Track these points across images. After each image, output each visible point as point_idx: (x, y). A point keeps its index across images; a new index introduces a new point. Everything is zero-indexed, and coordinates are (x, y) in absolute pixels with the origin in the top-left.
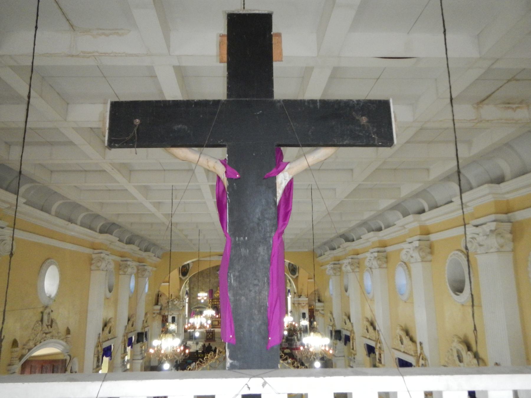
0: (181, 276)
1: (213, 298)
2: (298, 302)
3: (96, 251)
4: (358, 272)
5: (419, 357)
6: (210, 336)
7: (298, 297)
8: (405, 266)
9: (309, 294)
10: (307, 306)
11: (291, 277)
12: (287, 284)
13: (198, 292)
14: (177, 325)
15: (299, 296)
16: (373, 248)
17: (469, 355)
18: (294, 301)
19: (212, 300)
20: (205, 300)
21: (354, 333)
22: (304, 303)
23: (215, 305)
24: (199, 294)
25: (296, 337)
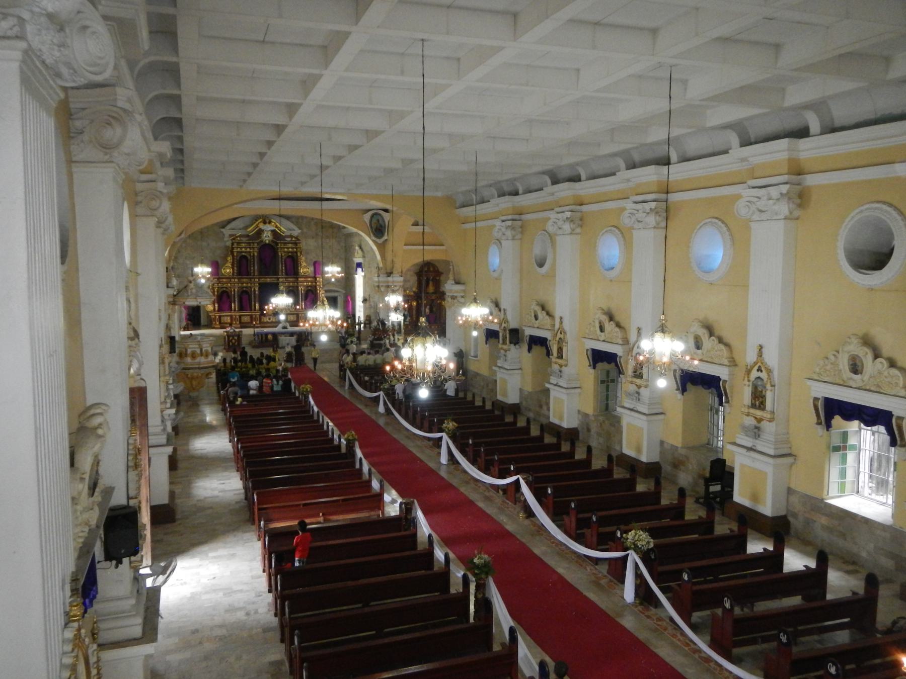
3: (144, 177)
4: (580, 234)
5: (752, 368)
6: (233, 341)
7: (386, 275)
8: (723, 225)
9: (404, 270)
11: (373, 241)
13: (196, 265)
15: (387, 273)
16: (637, 195)
17: (881, 362)
18: (379, 282)
21: (565, 333)
22: (396, 286)
23: (224, 289)
25: (387, 341)
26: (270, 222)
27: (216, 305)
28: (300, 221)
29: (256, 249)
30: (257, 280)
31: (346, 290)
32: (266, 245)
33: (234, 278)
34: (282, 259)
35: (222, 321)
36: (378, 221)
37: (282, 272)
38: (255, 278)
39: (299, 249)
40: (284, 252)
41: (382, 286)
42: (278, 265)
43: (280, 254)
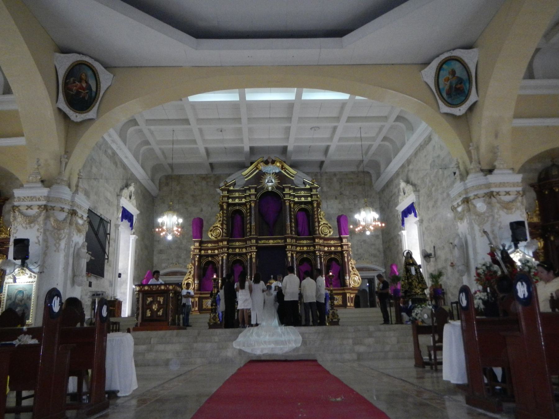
0: (63, 105)
1: (204, 240)
2: (486, 191)
6: (155, 307)
7: (482, 174)
10: (522, 203)
12: (399, 195)
13: (161, 214)
14: (41, 273)
15: (482, 170)
18: (466, 191)
19: (200, 245)
20: (174, 236)
22: (508, 193)
23: (210, 259)
24: (160, 220)
26: (273, 162)
27: (196, 282)
29: (253, 198)
30: (254, 241)
31: (385, 268)
33: (222, 241)
34: (290, 211)
35: (204, 307)
36: (453, 73)
37: (291, 230)
38: (250, 239)
39: (313, 197)
40: (295, 203)
41: (476, 196)
42: (286, 220)
43: (288, 204)
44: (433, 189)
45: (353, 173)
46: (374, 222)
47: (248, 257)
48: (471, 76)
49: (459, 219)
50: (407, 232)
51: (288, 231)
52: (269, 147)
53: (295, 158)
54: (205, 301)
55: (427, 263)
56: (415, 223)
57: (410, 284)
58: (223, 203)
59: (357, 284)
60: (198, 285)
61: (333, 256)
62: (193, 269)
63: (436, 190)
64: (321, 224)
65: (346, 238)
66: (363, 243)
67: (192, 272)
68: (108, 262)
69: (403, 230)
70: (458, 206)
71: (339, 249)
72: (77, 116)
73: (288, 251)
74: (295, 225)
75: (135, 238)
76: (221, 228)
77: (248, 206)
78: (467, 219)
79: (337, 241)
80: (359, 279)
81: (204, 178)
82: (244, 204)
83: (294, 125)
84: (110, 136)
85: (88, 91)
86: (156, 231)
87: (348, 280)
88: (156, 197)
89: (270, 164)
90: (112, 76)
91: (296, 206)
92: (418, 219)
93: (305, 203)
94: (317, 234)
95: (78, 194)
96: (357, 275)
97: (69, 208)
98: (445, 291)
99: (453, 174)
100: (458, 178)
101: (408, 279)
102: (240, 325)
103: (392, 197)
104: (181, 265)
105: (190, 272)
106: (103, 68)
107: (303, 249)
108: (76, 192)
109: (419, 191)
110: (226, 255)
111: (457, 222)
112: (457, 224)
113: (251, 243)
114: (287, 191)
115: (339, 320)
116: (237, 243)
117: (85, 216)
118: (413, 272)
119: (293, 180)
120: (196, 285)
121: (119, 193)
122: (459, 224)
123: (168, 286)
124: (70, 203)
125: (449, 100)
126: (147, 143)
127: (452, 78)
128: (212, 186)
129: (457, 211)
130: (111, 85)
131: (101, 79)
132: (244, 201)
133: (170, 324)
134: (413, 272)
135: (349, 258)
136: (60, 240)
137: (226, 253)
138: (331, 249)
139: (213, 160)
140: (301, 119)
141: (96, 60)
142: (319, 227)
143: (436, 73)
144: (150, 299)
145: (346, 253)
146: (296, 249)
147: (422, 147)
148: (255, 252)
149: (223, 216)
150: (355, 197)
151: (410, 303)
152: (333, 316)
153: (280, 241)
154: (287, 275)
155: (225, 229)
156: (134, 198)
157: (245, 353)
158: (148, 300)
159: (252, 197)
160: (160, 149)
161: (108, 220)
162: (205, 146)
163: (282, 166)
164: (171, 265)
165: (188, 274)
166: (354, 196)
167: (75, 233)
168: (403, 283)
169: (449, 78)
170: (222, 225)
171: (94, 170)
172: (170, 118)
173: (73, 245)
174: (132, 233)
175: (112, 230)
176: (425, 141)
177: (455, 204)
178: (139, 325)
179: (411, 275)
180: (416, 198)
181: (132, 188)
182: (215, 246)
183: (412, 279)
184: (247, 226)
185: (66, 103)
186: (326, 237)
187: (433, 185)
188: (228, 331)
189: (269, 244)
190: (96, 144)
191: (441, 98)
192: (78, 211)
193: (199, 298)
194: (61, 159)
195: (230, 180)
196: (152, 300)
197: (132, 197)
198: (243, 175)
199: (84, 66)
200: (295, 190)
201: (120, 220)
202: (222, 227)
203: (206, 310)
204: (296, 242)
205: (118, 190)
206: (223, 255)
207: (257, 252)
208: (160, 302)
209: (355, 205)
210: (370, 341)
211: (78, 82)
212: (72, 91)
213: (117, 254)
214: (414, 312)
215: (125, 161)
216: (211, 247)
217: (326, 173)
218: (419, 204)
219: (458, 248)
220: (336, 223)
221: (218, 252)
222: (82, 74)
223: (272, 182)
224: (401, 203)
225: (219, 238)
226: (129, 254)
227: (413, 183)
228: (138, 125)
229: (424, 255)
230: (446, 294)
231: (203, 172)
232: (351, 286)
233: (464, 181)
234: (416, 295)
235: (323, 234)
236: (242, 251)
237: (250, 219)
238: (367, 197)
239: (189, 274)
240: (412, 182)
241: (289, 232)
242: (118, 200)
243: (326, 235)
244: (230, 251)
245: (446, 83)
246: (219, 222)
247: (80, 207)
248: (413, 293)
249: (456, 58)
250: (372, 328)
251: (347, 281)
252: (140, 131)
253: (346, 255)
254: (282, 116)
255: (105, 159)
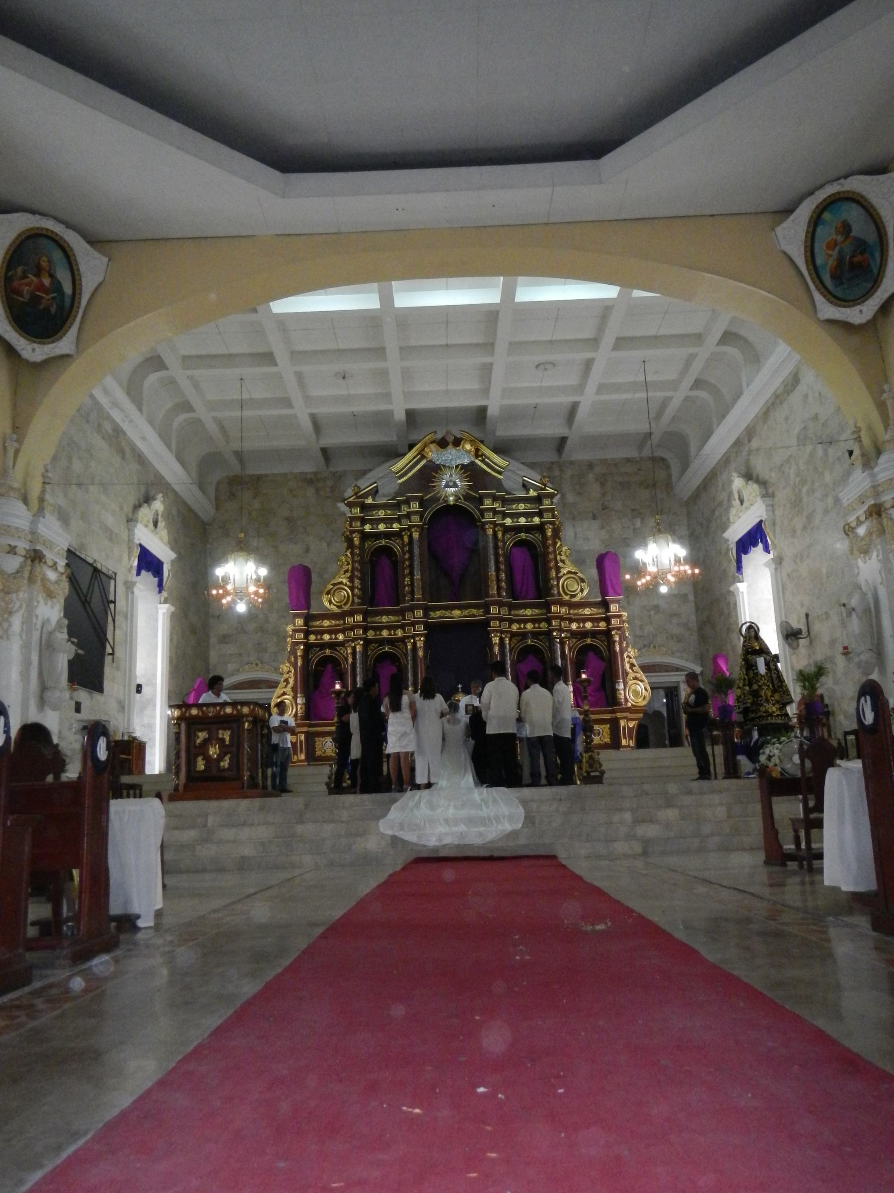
1: (313, 612)
6: (214, 751)
12: (730, 506)
13: (221, 559)
18: (876, 490)
19: (306, 623)
20: (252, 605)
23: (328, 652)
24: (220, 572)
26: (457, 442)
28: (557, 473)
29: (416, 520)
30: (419, 613)
31: (702, 666)
32: (448, 510)
33: (352, 613)
34: (496, 547)
35: (318, 753)
36: (846, 229)
37: (499, 588)
38: (412, 609)
40: (506, 529)
43: (490, 532)
44: (805, 489)
45: (629, 460)
46: (675, 565)
47: (409, 647)
48: (886, 235)
49: (861, 553)
50: (748, 586)
51: (492, 591)
52: (447, 410)
53: (503, 432)
54: (319, 741)
55: (791, 650)
56: (766, 565)
57: (756, 694)
58: (352, 532)
59: (640, 700)
60: (304, 707)
61: (589, 641)
62: (292, 674)
63: (812, 491)
64: (561, 574)
65: (618, 601)
66: (652, 613)
67: (291, 681)
68: (113, 661)
69: (740, 582)
70: (859, 523)
71: (603, 625)
72: (34, 350)
73: (493, 631)
74: (506, 576)
75: (168, 610)
76: (349, 587)
77: (406, 539)
78: (878, 551)
79: (599, 608)
80: (646, 689)
81: (310, 480)
82: (398, 534)
83: (500, 360)
84: (106, 392)
85: (55, 295)
86: (213, 596)
87: (622, 692)
88: (210, 524)
89: (450, 446)
90: (106, 260)
91: (509, 536)
92: (771, 556)
93: (528, 529)
94: (553, 595)
95: (44, 517)
96: (642, 681)
97: (28, 547)
98: (830, 709)
99: (847, 455)
100: (859, 463)
101: (750, 685)
102: (393, 787)
103: (714, 511)
104: (267, 667)
105: (287, 681)
106: (87, 246)
107: (525, 628)
108: (41, 511)
109: (773, 496)
110: (362, 642)
111: (856, 559)
112: (857, 564)
113: (414, 617)
114: (488, 503)
115: (603, 773)
116: (384, 617)
117: (62, 563)
118: (762, 669)
119: (499, 479)
120: (299, 707)
121: (130, 515)
122: (860, 562)
123: (239, 707)
124: (29, 537)
125: (839, 293)
126: (187, 407)
127: (845, 240)
128: (328, 497)
129: (856, 536)
130: (103, 282)
131: (83, 268)
132: (396, 526)
133: (245, 786)
134: (762, 669)
135: (624, 645)
136: (10, 613)
137: (361, 639)
138: (584, 627)
139: (331, 440)
140: (515, 347)
141: (69, 226)
142: (558, 579)
143: (807, 232)
144: (202, 735)
145: (616, 634)
146: (510, 627)
147: (777, 400)
148: (421, 635)
149: (353, 562)
150: (636, 513)
151: (756, 735)
152: (591, 766)
153: (474, 611)
154: (492, 680)
155: (358, 589)
156: (164, 527)
157: (404, 842)
158: (198, 738)
159: (412, 517)
160: (215, 419)
161: (110, 572)
162: (314, 411)
163: (477, 450)
164: (247, 667)
165: (282, 684)
166: (633, 510)
167: (41, 599)
168: (739, 692)
169: (836, 241)
170: (351, 579)
171: (77, 466)
172: (234, 351)
173: (39, 627)
174: (162, 600)
175: (118, 591)
176: (786, 385)
177: (852, 519)
178: (181, 788)
179: (757, 674)
180: (767, 510)
181: (158, 505)
182: (338, 625)
183: (760, 684)
184: (404, 581)
185: (10, 322)
186: (573, 600)
187: (804, 482)
188: (367, 800)
189: (453, 618)
190: (78, 410)
191: (820, 286)
192: (44, 552)
193: (307, 734)
194: (4, 443)
195: (365, 484)
196: (207, 736)
197: (159, 524)
198: (394, 472)
199: (45, 241)
200: (504, 501)
201: (134, 572)
202: (351, 585)
203: (324, 759)
204: (510, 614)
205: (128, 509)
206: (356, 643)
207: (426, 636)
208: (223, 740)
209: (635, 529)
210: (671, 814)
211: (35, 275)
212: (22, 296)
213: (131, 643)
214: (764, 753)
215: (141, 446)
216: (328, 627)
217: (572, 463)
218: (774, 524)
219: (857, 616)
220: (594, 572)
221: (345, 637)
222: (40, 258)
223: (455, 485)
224: (733, 523)
225: (346, 608)
226: (157, 644)
227: (760, 478)
228: (167, 369)
229: (785, 633)
230: (833, 715)
231: (308, 467)
232: (629, 705)
233: (872, 468)
234: (767, 717)
235: (566, 594)
236: (395, 634)
237: (411, 566)
238: (661, 512)
239: (285, 683)
240: (758, 476)
241: (495, 592)
242: (129, 530)
243: (573, 596)
244: (371, 634)
245: (830, 252)
246: (344, 574)
247: (50, 544)
248: (762, 714)
249: (850, 195)
250: (672, 788)
251: (620, 694)
252: (173, 382)
253: (617, 639)
254: (475, 340)
255: (99, 442)
